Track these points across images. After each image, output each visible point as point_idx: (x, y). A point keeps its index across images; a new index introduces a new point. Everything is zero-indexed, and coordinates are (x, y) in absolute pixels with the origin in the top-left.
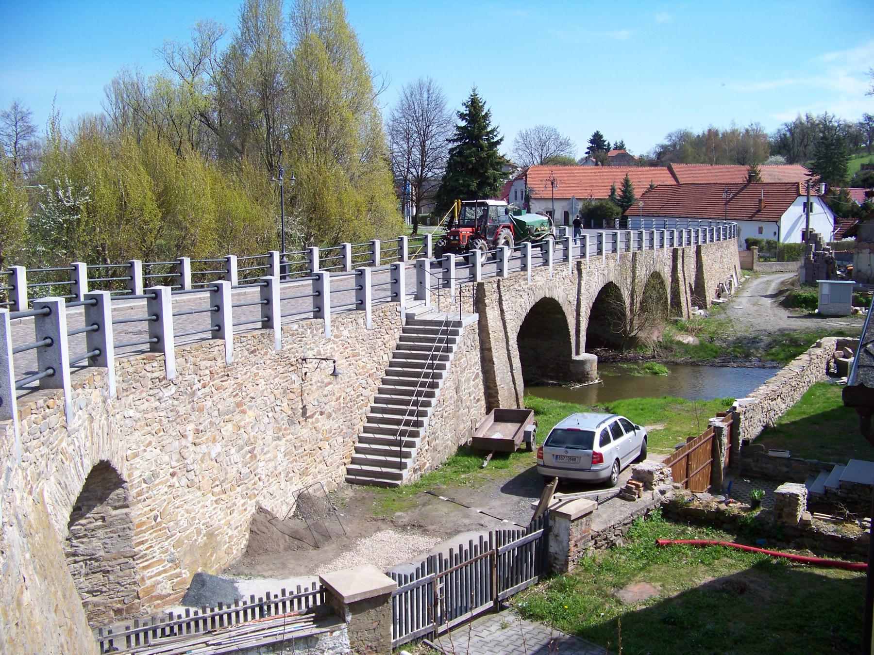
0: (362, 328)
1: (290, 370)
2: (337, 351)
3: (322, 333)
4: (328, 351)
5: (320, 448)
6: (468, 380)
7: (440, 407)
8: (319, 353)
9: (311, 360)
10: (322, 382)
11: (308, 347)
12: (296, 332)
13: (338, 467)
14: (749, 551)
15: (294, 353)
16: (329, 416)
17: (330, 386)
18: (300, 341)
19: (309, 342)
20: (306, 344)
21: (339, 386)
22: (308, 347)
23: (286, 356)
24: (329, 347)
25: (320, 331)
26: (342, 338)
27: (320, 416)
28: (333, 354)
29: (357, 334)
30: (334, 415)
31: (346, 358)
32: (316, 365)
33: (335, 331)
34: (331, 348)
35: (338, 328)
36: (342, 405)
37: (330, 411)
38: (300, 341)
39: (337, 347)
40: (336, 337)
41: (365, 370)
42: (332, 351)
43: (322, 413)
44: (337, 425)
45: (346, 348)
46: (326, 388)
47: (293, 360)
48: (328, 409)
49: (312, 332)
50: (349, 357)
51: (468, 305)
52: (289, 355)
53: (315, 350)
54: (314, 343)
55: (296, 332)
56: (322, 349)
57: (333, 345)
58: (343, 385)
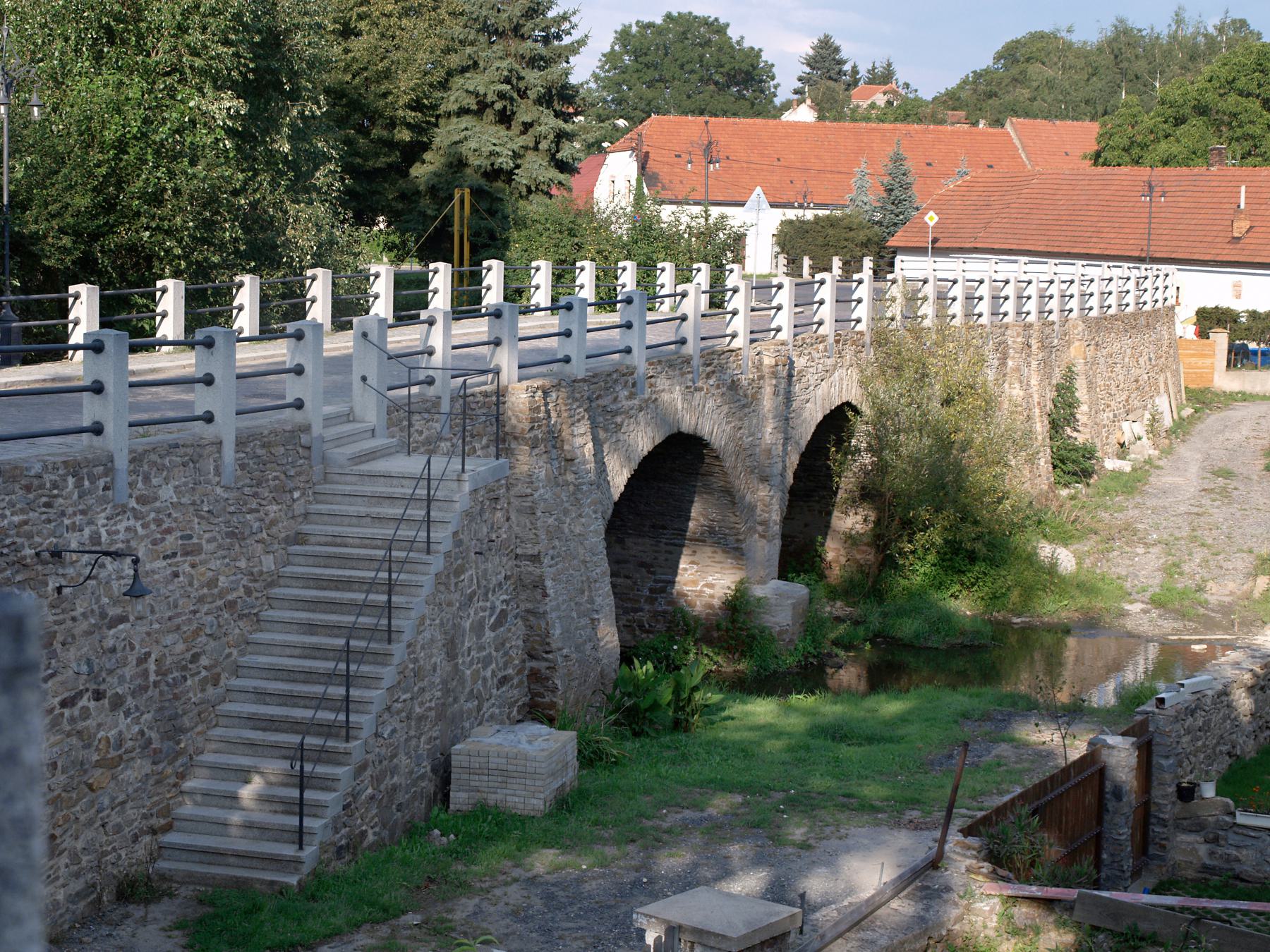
0: (208, 482)
1: (19, 578)
2: (142, 538)
3: (106, 488)
4: (121, 536)
5: (90, 787)
6: (478, 628)
7: (405, 692)
8: (96, 538)
9: (74, 556)
10: (103, 615)
11: (67, 522)
12: (36, 482)
13: (136, 839)
14: (53, 380)
15: (30, 536)
16: (117, 702)
17: (121, 627)
18: (47, 505)
19: (70, 510)
20: (63, 514)
21: (145, 629)
22: (67, 522)
23: (8, 541)
24: (121, 527)
25: (101, 483)
26: (158, 504)
27: (92, 704)
28: (133, 544)
29: (196, 498)
30: (130, 702)
31: (165, 558)
32: (87, 571)
33: (140, 485)
34: (128, 529)
35: (147, 479)
36: (152, 678)
37: (119, 690)
38: (47, 505)
39: (144, 526)
40: (142, 500)
41: (216, 591)
42: (130, 536)
43: (98, 696)
44: (136, 729)
45: (168, 531)
46: (112, 632)
47: (29, 552)
48: (114, 686)
49: (79, 485)
50: (174, 555)
51: (484, 441)
52: (19, 540)
53: (87, 532)
54: (83, 512)
55: (36, 482)
56: (103, 531)
57: (132, 522)
58: (156, 626)
